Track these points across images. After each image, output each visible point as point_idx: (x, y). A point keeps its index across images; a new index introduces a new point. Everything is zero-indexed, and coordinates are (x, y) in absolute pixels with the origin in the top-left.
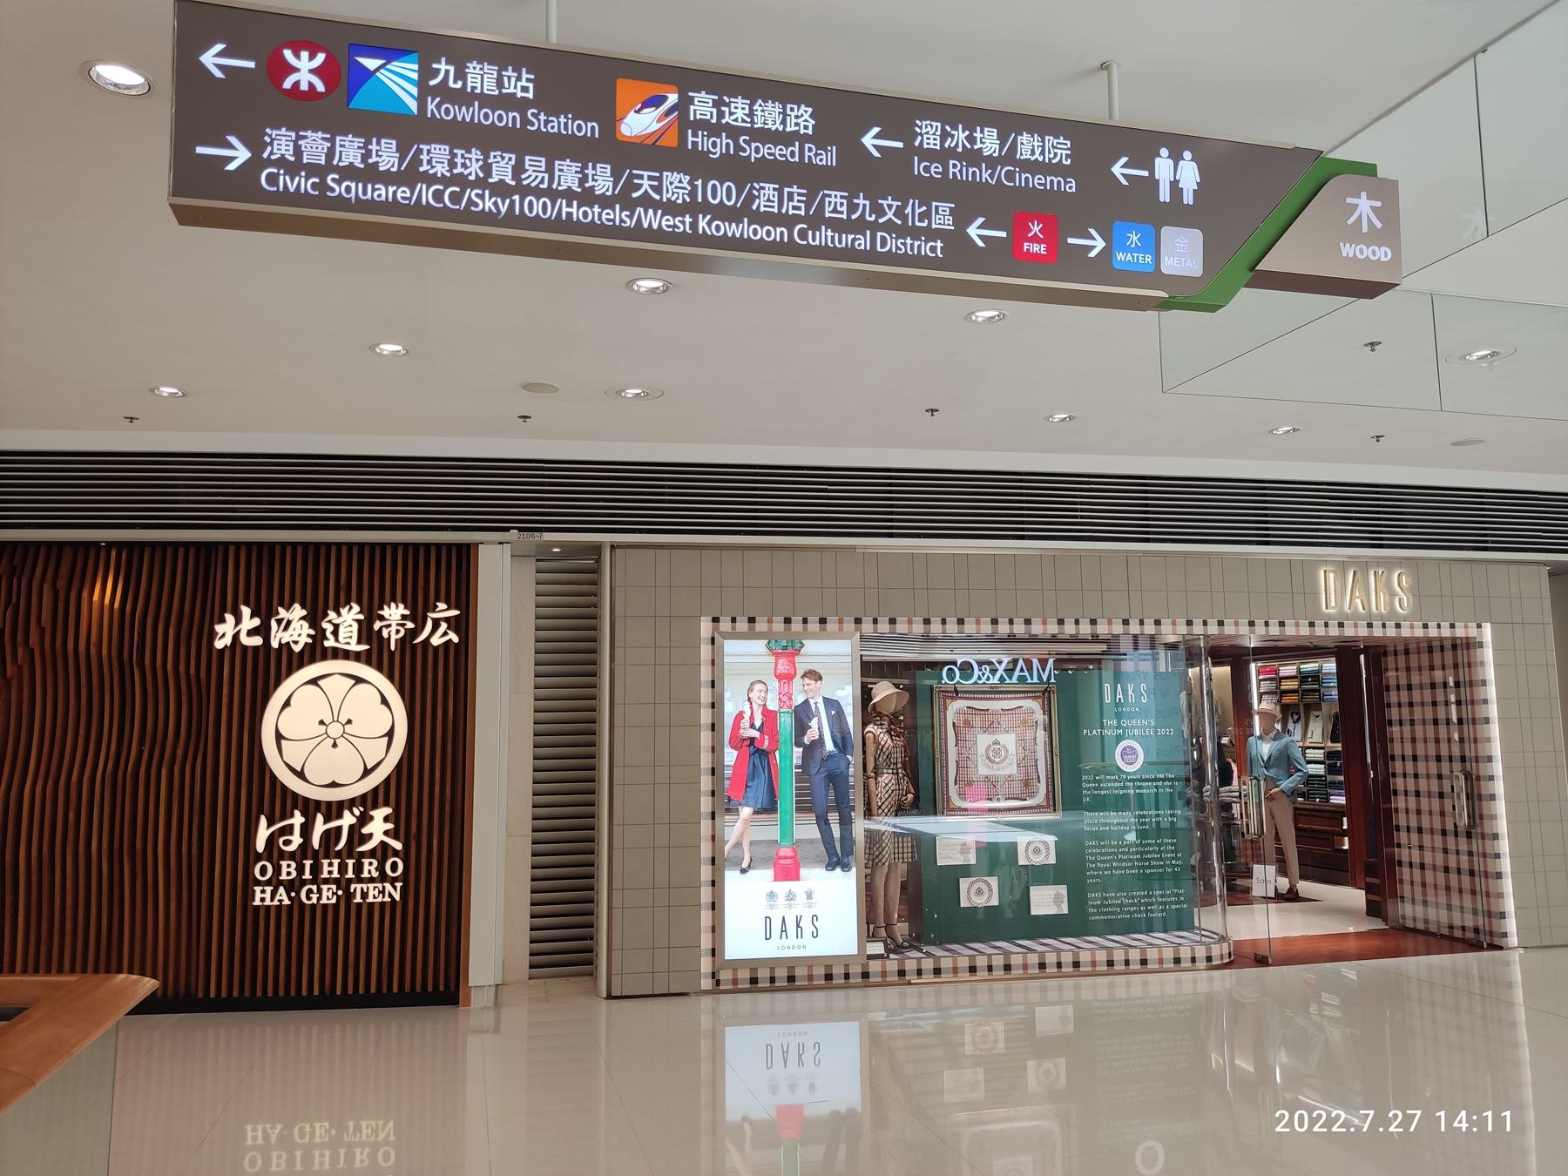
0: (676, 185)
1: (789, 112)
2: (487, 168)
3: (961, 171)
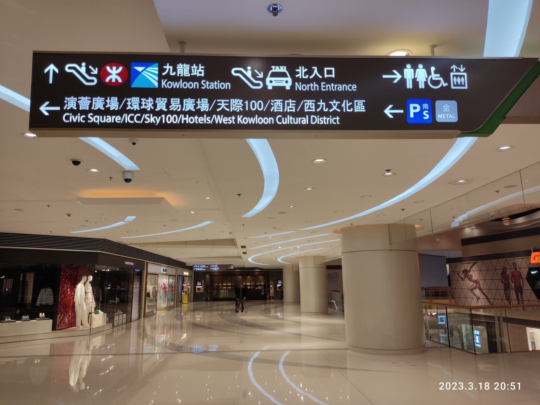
0: (236, 104)
2: (155, 105)
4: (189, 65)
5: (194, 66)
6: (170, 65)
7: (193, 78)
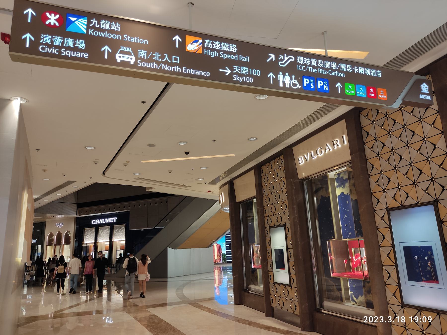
1: (230, 46)
3: (321, 71)
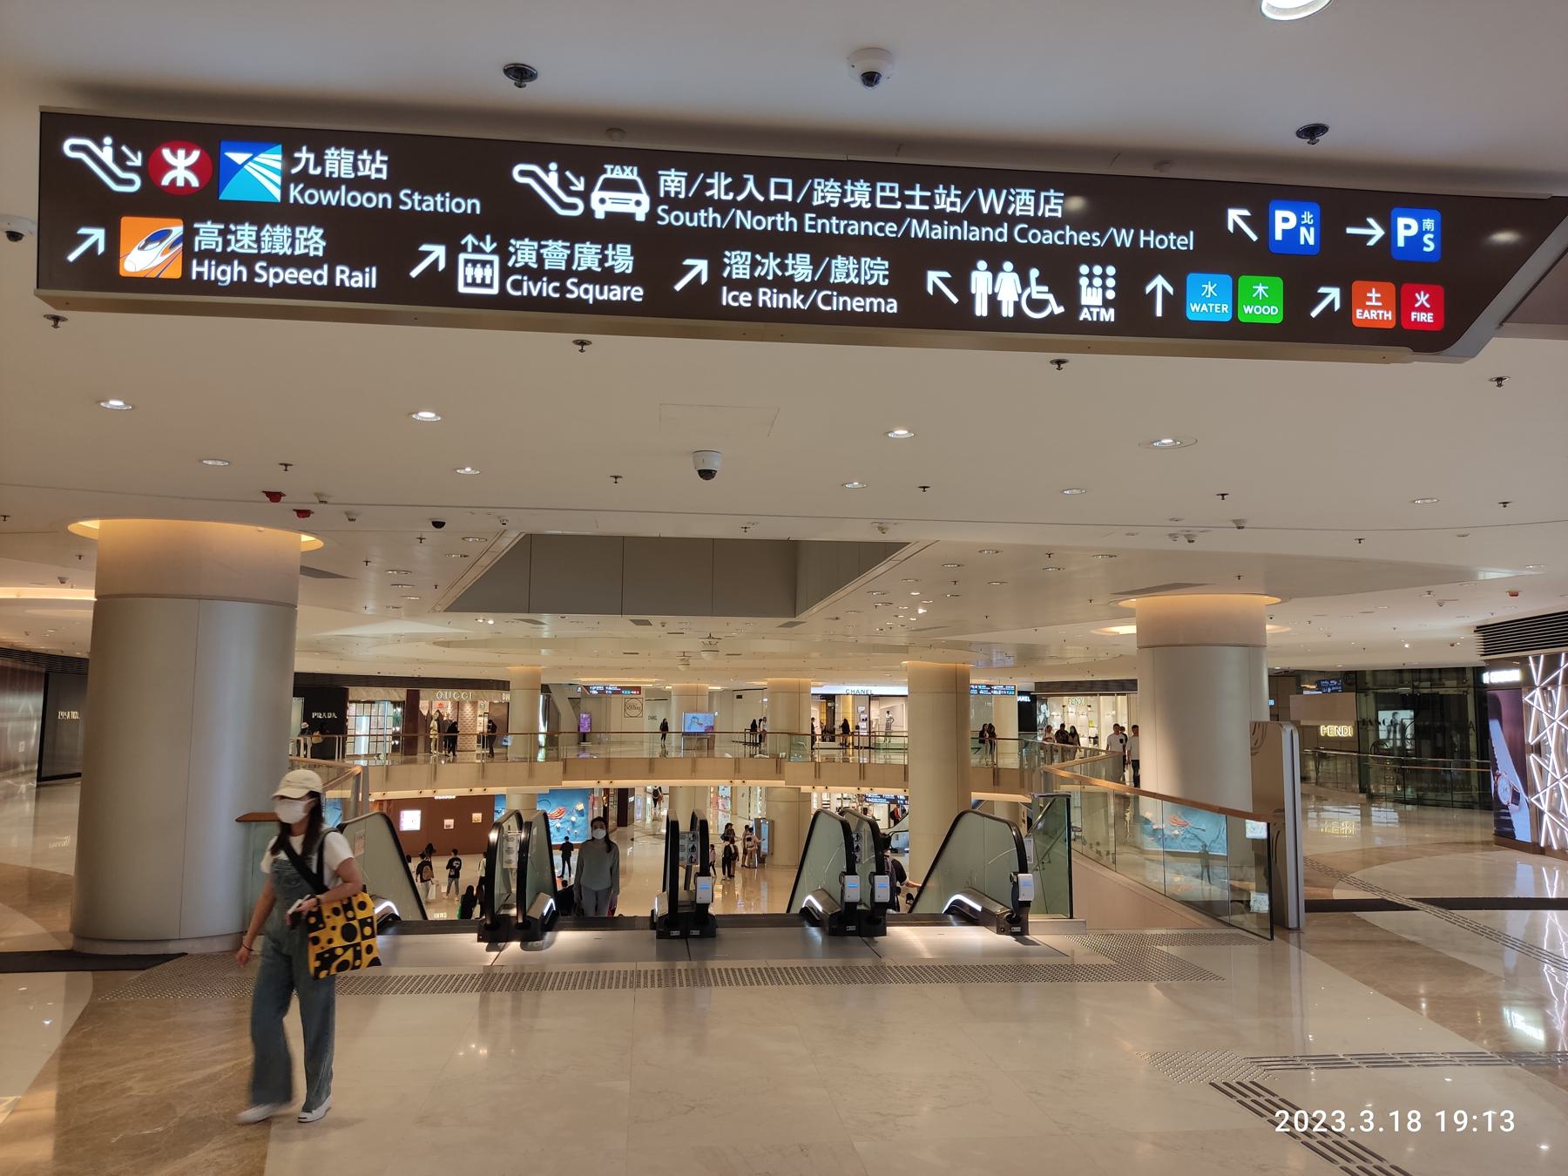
4: (353, 153)
5: (365, 155)
6: (309, 151)
7: (361, 184)
